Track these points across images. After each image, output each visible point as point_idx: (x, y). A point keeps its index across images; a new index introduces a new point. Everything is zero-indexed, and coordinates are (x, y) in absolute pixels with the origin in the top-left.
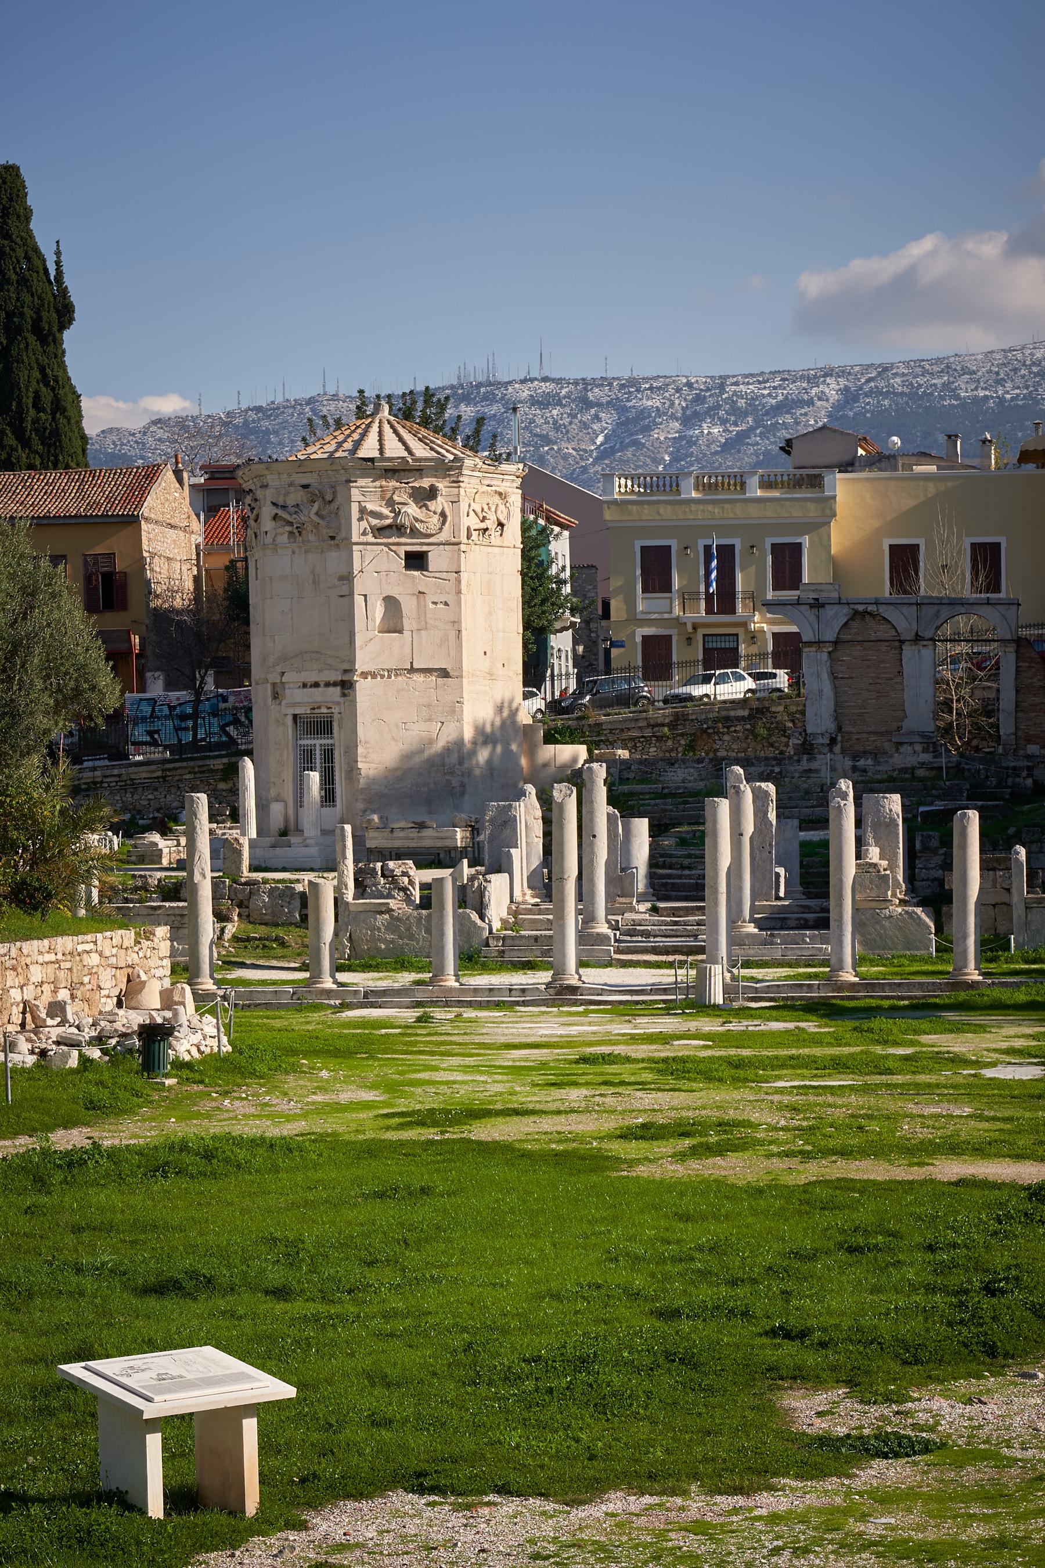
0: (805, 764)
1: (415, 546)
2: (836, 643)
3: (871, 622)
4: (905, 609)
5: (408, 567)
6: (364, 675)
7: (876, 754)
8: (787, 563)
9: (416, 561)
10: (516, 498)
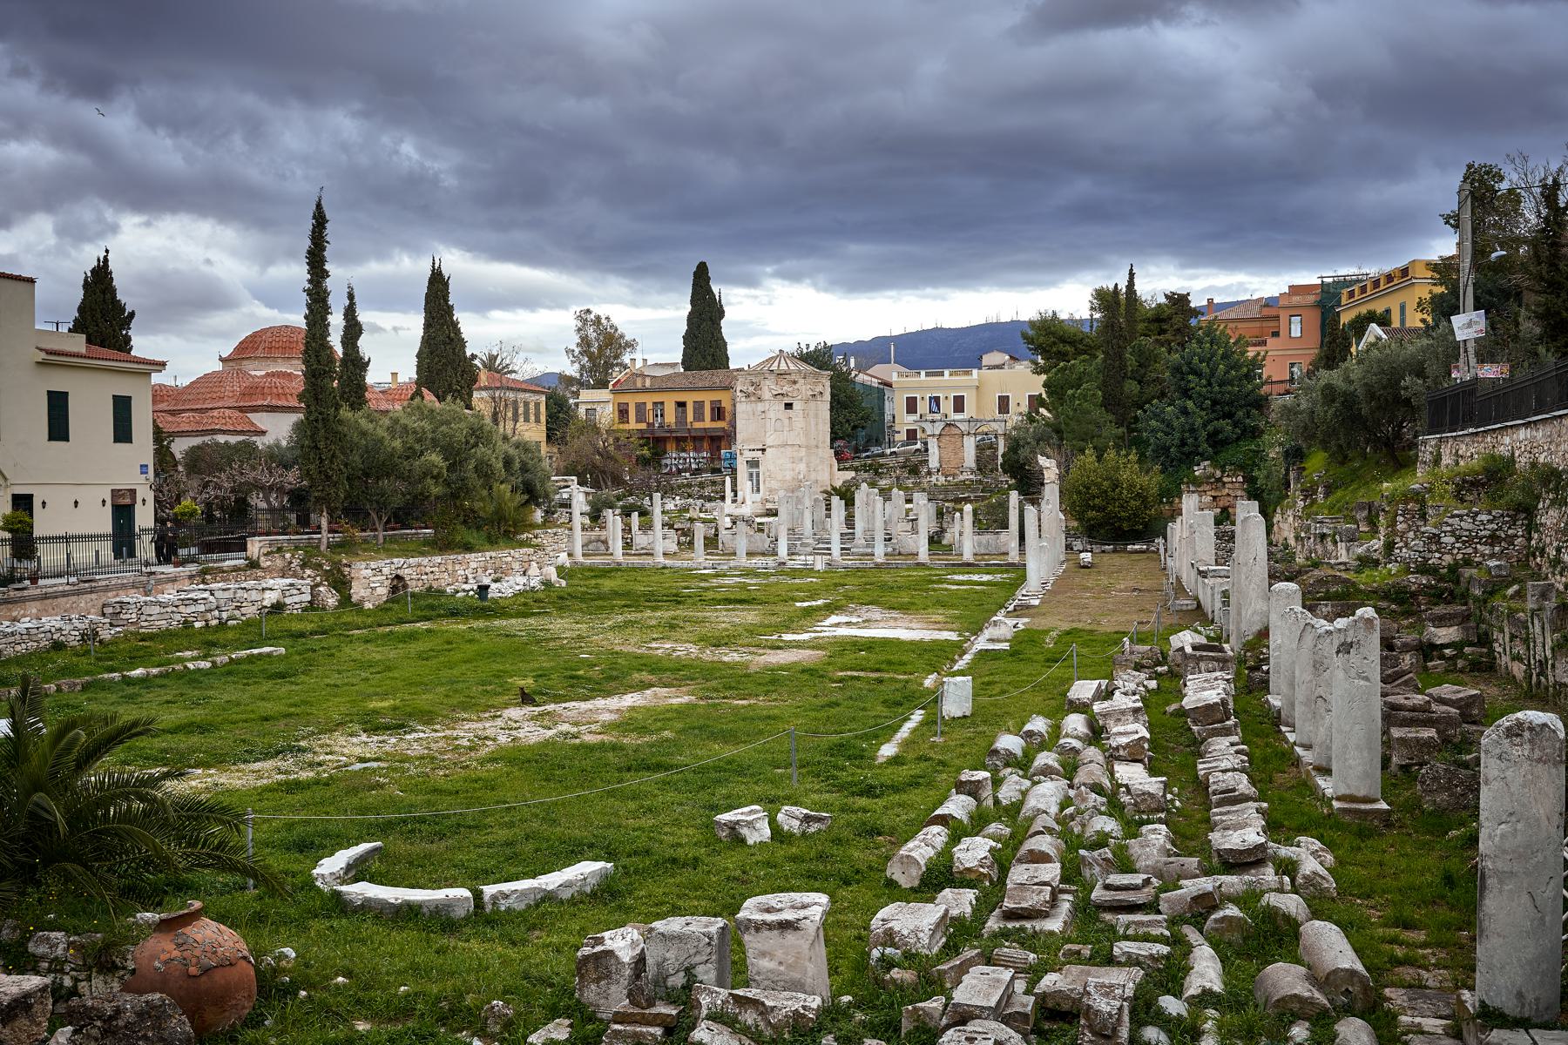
7: (954, 475)
8: (959, 404)
9: (789, 406)
10: (828, 384)
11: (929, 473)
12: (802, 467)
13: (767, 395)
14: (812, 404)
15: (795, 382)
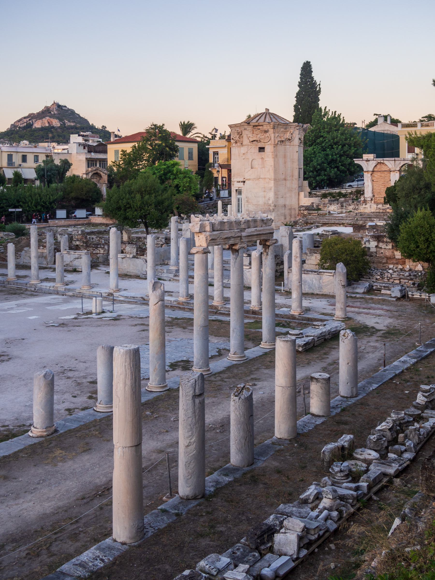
0: (364, 206)
1: (260, 145)
2: (373, 171)
3: (383, 166)
4: (391, 162)
5: (259, 151)
6: (249, 180)
9: (262, 149)
11: (365, 202)
12: (271, 195)
13: (246, 141)
14: (281, 148)
15: (266, 132)
